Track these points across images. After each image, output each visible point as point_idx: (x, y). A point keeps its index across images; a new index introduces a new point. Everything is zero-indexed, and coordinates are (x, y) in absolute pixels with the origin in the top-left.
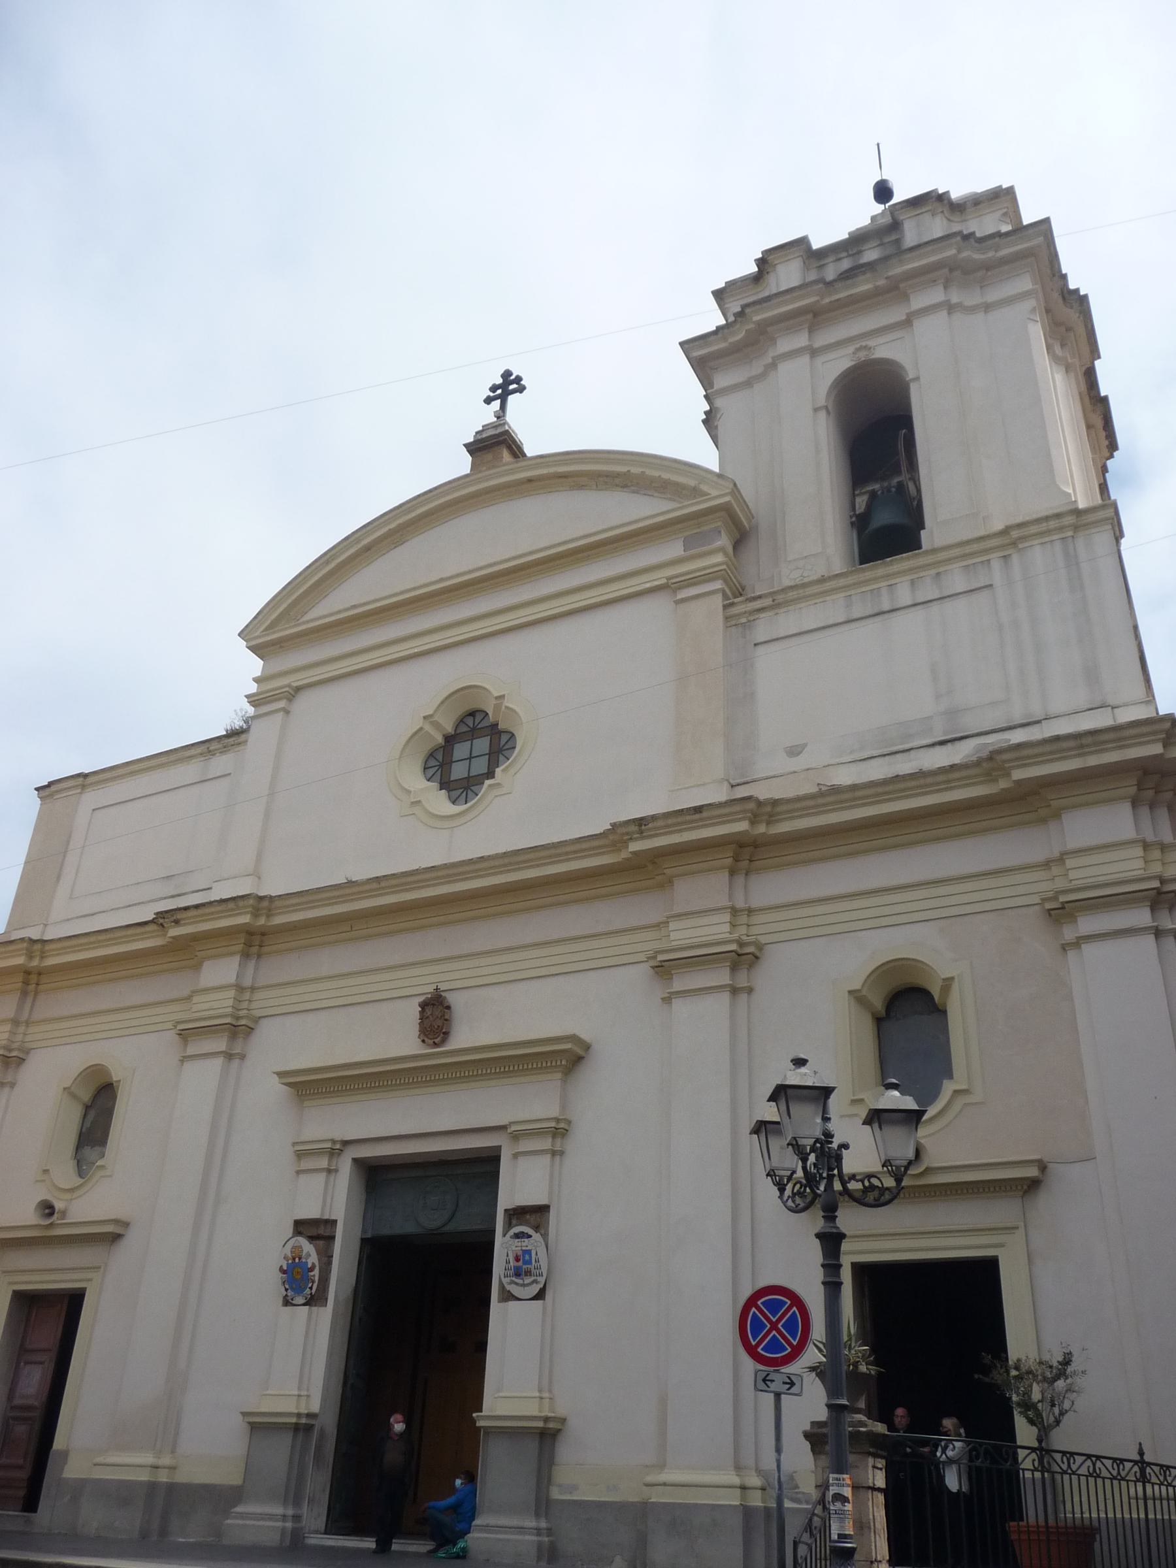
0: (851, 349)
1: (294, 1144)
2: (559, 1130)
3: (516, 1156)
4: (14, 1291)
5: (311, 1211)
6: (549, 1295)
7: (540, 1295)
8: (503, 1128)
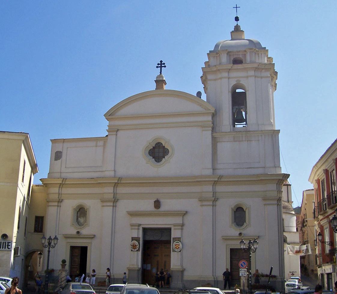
0: (236, 79)
2: (183, 225)
4: (70, 246)
6: (181, 251)
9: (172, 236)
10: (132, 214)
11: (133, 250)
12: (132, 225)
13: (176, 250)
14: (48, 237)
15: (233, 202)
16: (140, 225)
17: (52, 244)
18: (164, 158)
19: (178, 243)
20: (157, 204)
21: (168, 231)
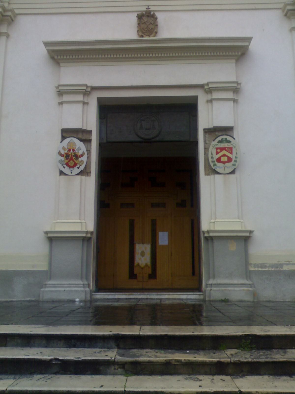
1: (57, 87)
3: (210, 101)
6: (237, 172)
7: (233, 172)
8: (201, 86)
11: (67, 170)
13: (219, 167)
19: (229, 142)
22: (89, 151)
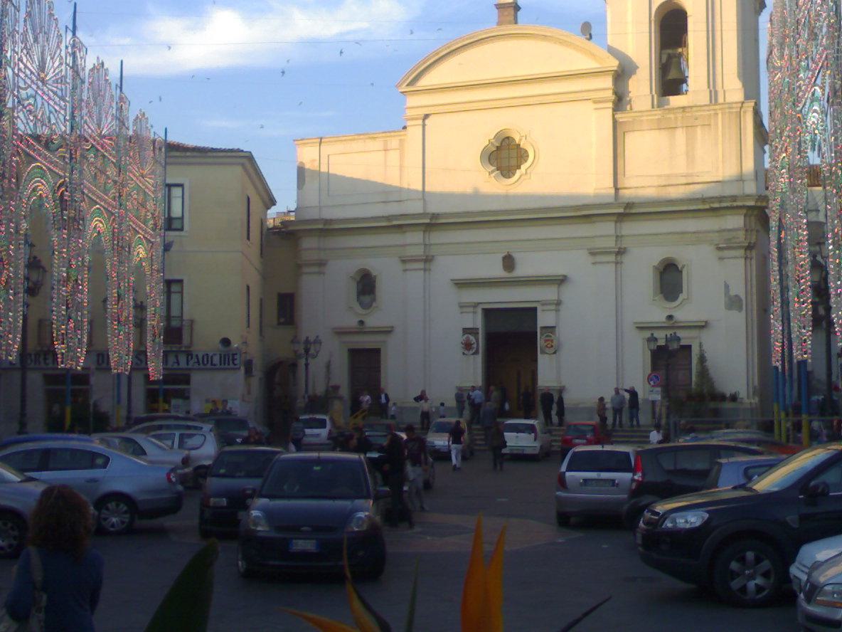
2: (559, 303)
5: (470, 325)
7: (555, 353)
9: (539, 326)
10: (462, 284)
12: (462, 306)
14: (303, 339)
15: (658, 255)
16: (476, 305)
17: (312, 351)
18: (520, 168)
19: (551, 336)
20: (509, 262)
21: (530, 313)
22: (477, 340)
